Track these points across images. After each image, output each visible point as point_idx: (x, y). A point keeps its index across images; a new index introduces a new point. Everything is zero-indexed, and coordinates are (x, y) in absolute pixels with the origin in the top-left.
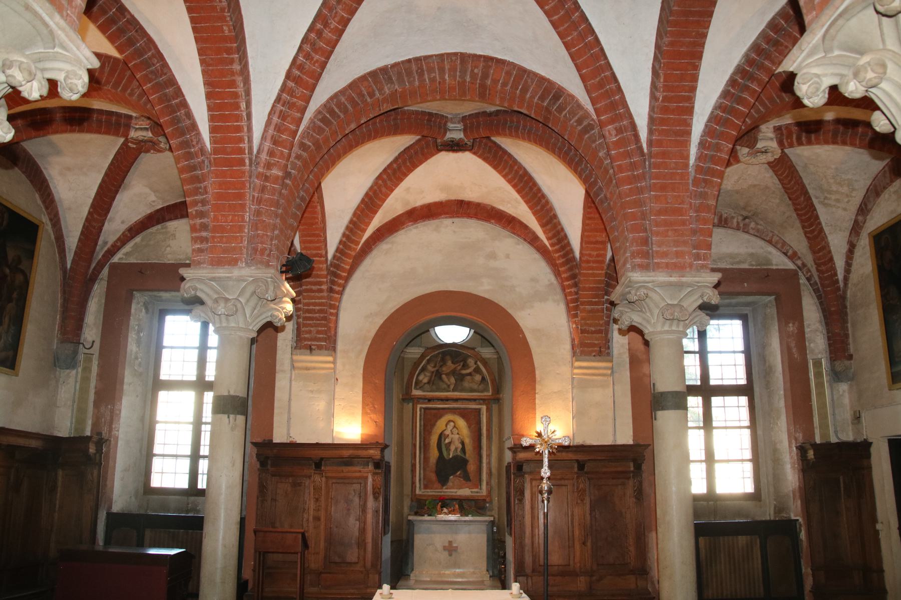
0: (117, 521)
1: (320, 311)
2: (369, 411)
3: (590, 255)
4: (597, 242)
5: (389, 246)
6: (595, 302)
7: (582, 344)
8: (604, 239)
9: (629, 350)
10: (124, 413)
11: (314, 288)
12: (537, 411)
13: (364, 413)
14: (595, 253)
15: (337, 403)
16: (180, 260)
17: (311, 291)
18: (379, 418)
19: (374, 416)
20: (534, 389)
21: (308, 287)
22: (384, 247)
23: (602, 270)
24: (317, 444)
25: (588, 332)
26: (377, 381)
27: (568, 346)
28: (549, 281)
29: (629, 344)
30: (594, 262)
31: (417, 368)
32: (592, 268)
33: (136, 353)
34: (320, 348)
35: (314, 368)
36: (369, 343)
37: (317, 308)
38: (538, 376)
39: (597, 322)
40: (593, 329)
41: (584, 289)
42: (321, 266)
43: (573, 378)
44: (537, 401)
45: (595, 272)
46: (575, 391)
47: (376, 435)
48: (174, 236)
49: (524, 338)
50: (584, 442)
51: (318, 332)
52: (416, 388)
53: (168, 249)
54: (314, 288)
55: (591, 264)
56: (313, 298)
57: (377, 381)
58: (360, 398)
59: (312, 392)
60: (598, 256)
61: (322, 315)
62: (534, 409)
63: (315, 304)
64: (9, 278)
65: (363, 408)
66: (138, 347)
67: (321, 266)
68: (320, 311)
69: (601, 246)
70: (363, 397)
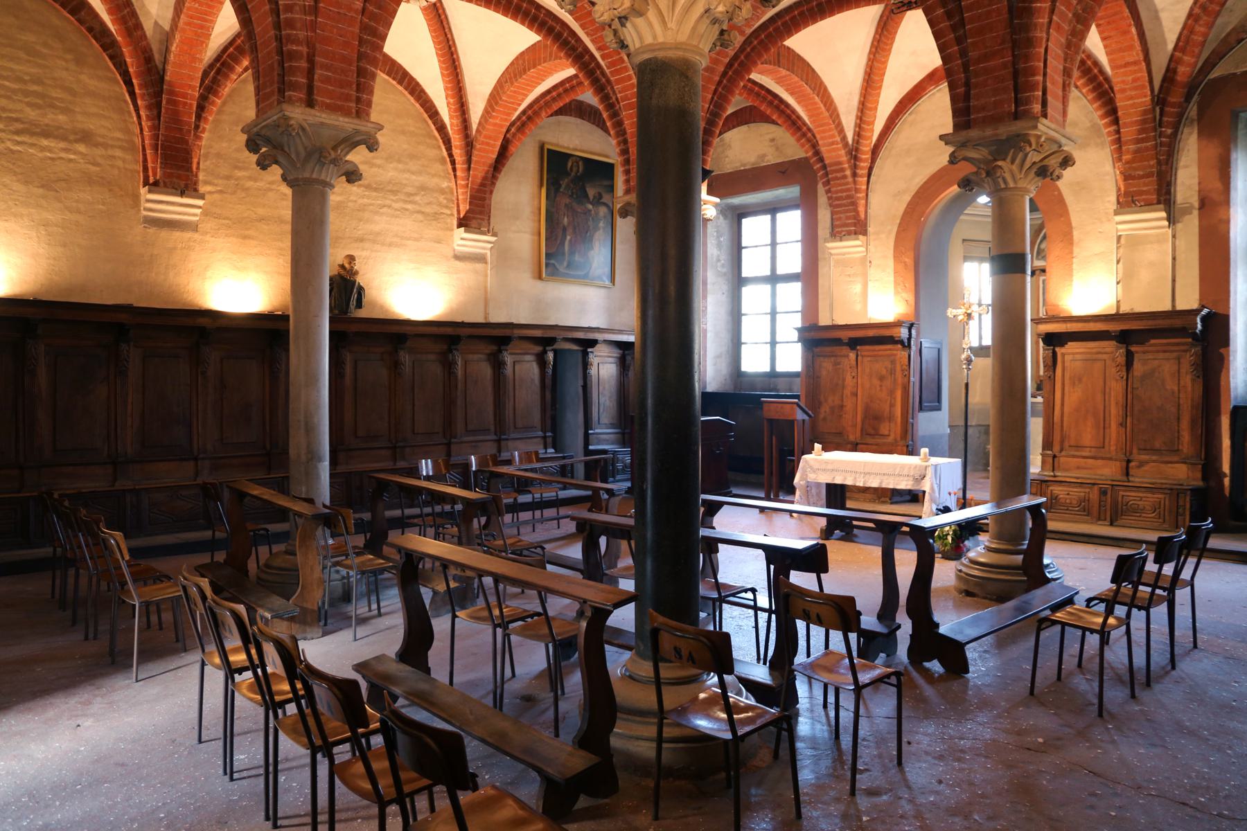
0: (712, 401)
1: (848, 197)
2: (900, 290)
3: (1123, 82)
4: (1127, 65)
5: (913, 116)
6: (1142, 139)
7: (1126, 194)
8: (1137, 58)
9: (1200, 191)
10: (710, 309)
11: (839, 175)
12: (1074, 278)
13: (897, 293)
14: (1130, 78)
15: (870, 284)
16: (737, 167)
17: (837, 178)
18: (910, 297)
19: (905, 295)
20: (1071, 252)
21: (834, 175)
22: (907, 117)
23: (1145, 96)
24: (846, 325)
25: (1133, 178)
26: (907, 260)
27: (1113, 198)
28: (1090, 121)
29: (1199, 183)
30: (1131, 89)
31: (1039, 235)
32: (1131, 98)
33: (718, 256)
34: (849, 233)
35: (849, 253)
36: (898, 221)
37: (845, 194)
38: (1075, 238)
39: (1146, 163)
40: (1141, 173)
41: (1126, 125)
42: (840, 153)
43: (1119, 238)
44: (1074, 266)
45: (1136, 101)
46: (1121, 250)
47: (907, 314)
48: (730, 146)
49: (1060, 194)
50: (1132, 309)
51: (848, 218)
52: (1037, 258)
53: (727, 159)
54: (839, 175)
55: (1129, 93)
56: (840, 185)
57: (907, 260)
58: (892, 279)
59: (849, 276)
60: (1134, 80)
61: (849, 201)
62: (1071, 275)
63: (842, 191)
64: (593, 212)
65: (895, 287)
66: (720, 250)
67: (840, 153)
68: (848, 197)
69: (1136, 68)
70: (895, 277)
